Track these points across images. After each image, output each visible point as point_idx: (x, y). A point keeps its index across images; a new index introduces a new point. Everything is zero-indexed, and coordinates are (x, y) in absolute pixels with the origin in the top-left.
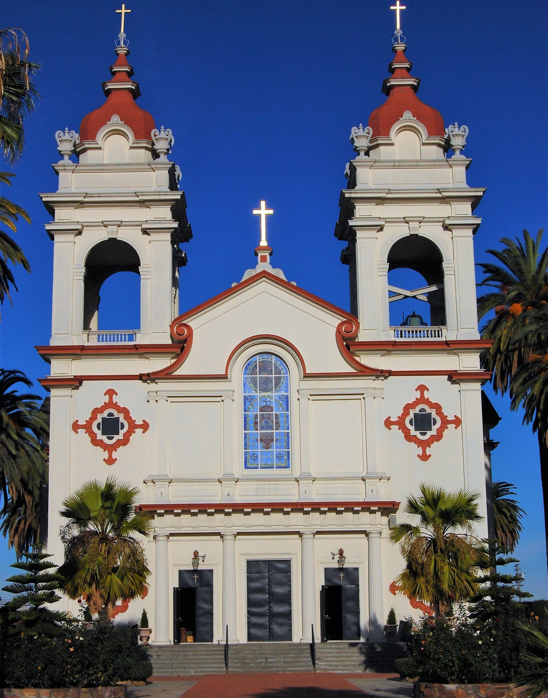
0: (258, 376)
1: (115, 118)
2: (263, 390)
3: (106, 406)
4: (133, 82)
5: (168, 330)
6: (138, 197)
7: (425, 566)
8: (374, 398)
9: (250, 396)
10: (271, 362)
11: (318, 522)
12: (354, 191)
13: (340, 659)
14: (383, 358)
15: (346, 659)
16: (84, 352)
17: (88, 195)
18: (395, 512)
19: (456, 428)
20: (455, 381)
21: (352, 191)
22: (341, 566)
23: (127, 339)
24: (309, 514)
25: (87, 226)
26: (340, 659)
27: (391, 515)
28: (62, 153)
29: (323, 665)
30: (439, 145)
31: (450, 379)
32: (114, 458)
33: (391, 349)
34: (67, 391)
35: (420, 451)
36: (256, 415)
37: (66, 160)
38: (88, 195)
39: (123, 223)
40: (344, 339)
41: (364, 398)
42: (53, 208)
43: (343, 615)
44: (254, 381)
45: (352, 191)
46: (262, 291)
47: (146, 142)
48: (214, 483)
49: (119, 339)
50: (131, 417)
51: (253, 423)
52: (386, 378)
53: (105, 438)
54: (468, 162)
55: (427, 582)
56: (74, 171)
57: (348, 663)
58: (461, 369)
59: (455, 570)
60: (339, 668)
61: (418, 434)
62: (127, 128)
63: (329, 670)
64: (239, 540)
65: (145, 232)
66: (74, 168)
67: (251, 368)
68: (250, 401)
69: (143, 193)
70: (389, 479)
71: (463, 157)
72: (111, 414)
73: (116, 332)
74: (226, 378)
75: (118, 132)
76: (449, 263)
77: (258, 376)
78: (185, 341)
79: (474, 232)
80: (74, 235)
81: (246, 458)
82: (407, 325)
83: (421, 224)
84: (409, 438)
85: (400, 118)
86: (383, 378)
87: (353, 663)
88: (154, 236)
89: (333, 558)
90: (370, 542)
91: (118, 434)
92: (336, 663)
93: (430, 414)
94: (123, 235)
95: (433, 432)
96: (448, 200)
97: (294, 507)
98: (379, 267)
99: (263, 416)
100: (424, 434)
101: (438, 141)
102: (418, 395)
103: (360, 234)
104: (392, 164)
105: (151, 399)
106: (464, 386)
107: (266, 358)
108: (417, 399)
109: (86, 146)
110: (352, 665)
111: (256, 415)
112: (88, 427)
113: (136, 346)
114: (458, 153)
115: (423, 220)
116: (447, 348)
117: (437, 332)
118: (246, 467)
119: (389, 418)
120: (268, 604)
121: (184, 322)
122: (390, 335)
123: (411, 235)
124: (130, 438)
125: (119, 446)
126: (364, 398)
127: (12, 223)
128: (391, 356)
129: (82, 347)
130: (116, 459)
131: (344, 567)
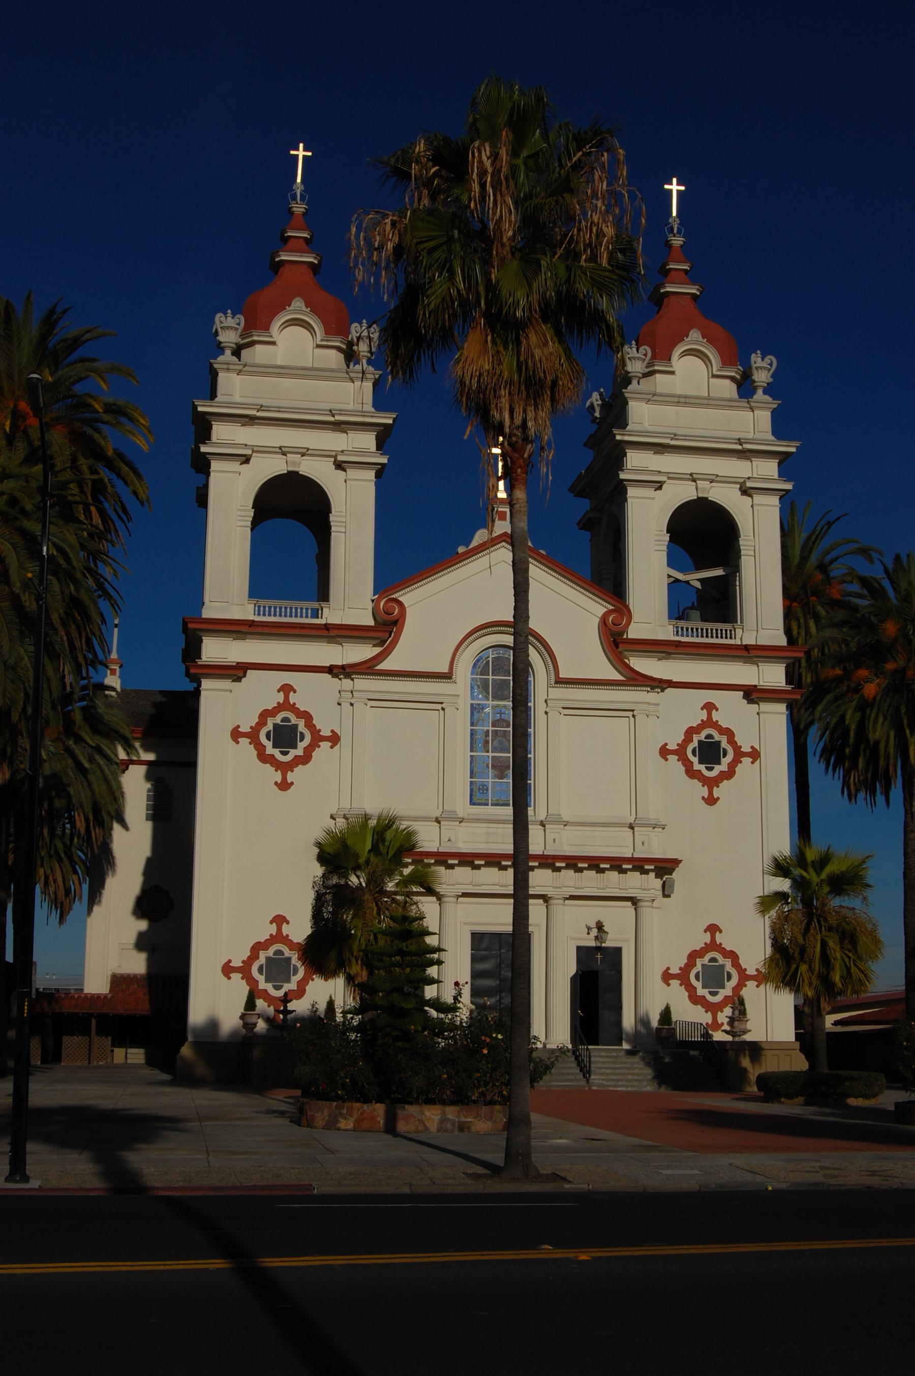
0: (491, 677)
1: (298, 303)
2: (495, 697)
3: (279, 708)
4: (317, 255)
5: (370, 605)
6: (333, 416)
7: (808, 949)
9: (479, 705)
10: (510, 659)
11: (572, 883)
13: (618, 1071)
15: (626, 1071)
16: (251, 630)
17: (263, 408)
18: (671, 874)
19: (752, 763)
20: (752, 699)
22: (599, 944)
23: (309, 615)
24: (560, 871)
25: (258, 452)
26: (618, 1071)
27: (666, 876)
28: (222, 345)
29: (599, 1079)
31: (745, 697)
32: (289, 782)
33: (671, 651)
34: (226, 684)
35: (705, 792)
36: (488, 731)
37: (228, 356)
38: (263, 408)
39: (310, 452)
41: (634, 716)
42: (210, 421)
43: (600, 1011)
44: (485, 684)
46: (501, 560)
47: (340, 339)
48: (429, 823)
49: (294, 614)
50: (314, 725)
51: (482, 742)
52: (663, 690)
53: (276, 753)
54: (775, 406)
55: (811, 970)
56: (240, 372)
57: (630, 1077)
58: (762, 683)
59: (850, 955)
60: (620, 1083)
61: (702, 768)
62: (313, 317)
63: (608, 1086)
64: (462, 903)
65: (340, 466)
66: (242, 366)
67: (482, 666)
68: (479, 712)
69: (342, 412)
70: (664, 829)
71: (768, 398)
72: (285, 720)
73: (278, 603)
74: (450, 678)
75: (299, 323)
77: (491, 677)
78: (395, 623)
80: (239, 463)
81: (472, 791)
82: (683, 619)
83: (713, 484)
84: (691, 773)
85: (685, 338)
86: (659, 690)
87: (636, 1078)
88: (352, 473)
89: (588, 933)
90: (550, 910)
91: (295, 747)
92: (614, 1077)
94: (310, 468)
95: (723, 767)
96: (748, 454)
97: (543, 861)
99: (496, 733)
102: (704, 715)
103: (631, 492)
104: (676, 400)
105: (344, 702)
106: (765, 707)
107: (502, 654)
108: (702, 721)
109: (255, 338)
110: (636, 1080)
111: (488, 731)
112: (253, 736)
113: (328, 626)
114: (760, 392)
115: (716, 479)
116: (745, 653)
117: (728, 632)
118: (472, 803)
119: (666, 744)
120: (498, 993)
121: (394, 596)
122: (666, 632)
123: (698, 498)
124: (313, 754)
125: (297, 765)
126: (634, 716)
127: (141, 439)
128: (670, 660)
129: (251, 622)
130: (292, 783)
131: (603, 945)
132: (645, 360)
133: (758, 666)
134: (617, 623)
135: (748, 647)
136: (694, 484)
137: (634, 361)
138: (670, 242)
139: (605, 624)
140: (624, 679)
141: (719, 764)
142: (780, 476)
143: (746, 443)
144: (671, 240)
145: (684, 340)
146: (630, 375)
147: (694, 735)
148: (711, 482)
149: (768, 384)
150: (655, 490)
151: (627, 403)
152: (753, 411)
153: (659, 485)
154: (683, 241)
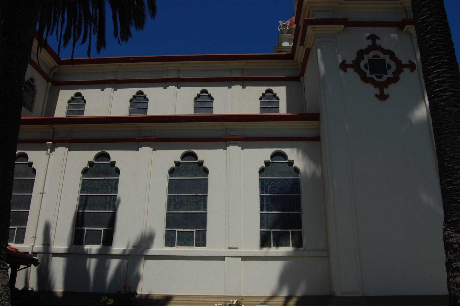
35: (377, 91)
93: (384, 61)
95: (390, 74)
100: (381, 77)
141: (386, 73)
147: (365, 55)
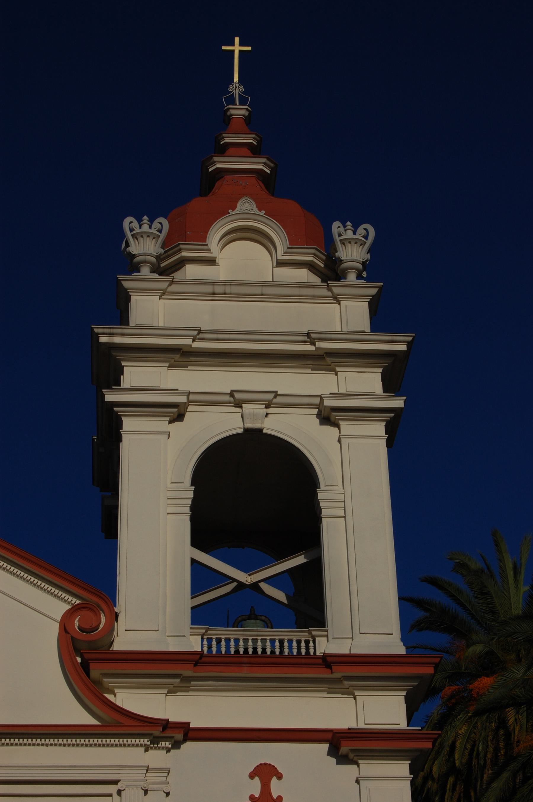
8: (146, 792)
12: (119, 331)
14: (172, 698)
21: (115, 331)
30: (311, 267)
31: (334, 752)
40: (78, 651)
45: (115, 331)
52: (177, 745)
54: (374, 291)
76: (333, 492)
79: (390, 429)
83: (270, 410)
85: (230, 211)
86: (168, 745)
96: (329, 360)
98: (170, 494)
101: (310, 258)
104: (209, 289)
114: (352, 277)
115: (275, 401)
116: (325, 674)
117: (303, 644)
123: (247, 430)
126: (119, 792)
132: (159, 236)
133: (355, 698)
134: (86, 626)
135: (329, 659)
136: (239, 410)
137: (141, 240)
138: (228, 113)
139: (66, 631)
140: (97, 723)
142: (385, 391)
143: (320, 339)
144: (229, 109)
145: (229, 213)
146: (136, 260)
148: (266, 407)
149: (363, 264)
150: (170, 422)
151: (128, 299)
152: (339, 304)
153: (176, 410)
154: (247, 109)
